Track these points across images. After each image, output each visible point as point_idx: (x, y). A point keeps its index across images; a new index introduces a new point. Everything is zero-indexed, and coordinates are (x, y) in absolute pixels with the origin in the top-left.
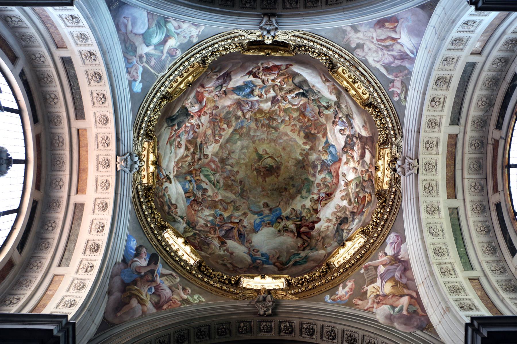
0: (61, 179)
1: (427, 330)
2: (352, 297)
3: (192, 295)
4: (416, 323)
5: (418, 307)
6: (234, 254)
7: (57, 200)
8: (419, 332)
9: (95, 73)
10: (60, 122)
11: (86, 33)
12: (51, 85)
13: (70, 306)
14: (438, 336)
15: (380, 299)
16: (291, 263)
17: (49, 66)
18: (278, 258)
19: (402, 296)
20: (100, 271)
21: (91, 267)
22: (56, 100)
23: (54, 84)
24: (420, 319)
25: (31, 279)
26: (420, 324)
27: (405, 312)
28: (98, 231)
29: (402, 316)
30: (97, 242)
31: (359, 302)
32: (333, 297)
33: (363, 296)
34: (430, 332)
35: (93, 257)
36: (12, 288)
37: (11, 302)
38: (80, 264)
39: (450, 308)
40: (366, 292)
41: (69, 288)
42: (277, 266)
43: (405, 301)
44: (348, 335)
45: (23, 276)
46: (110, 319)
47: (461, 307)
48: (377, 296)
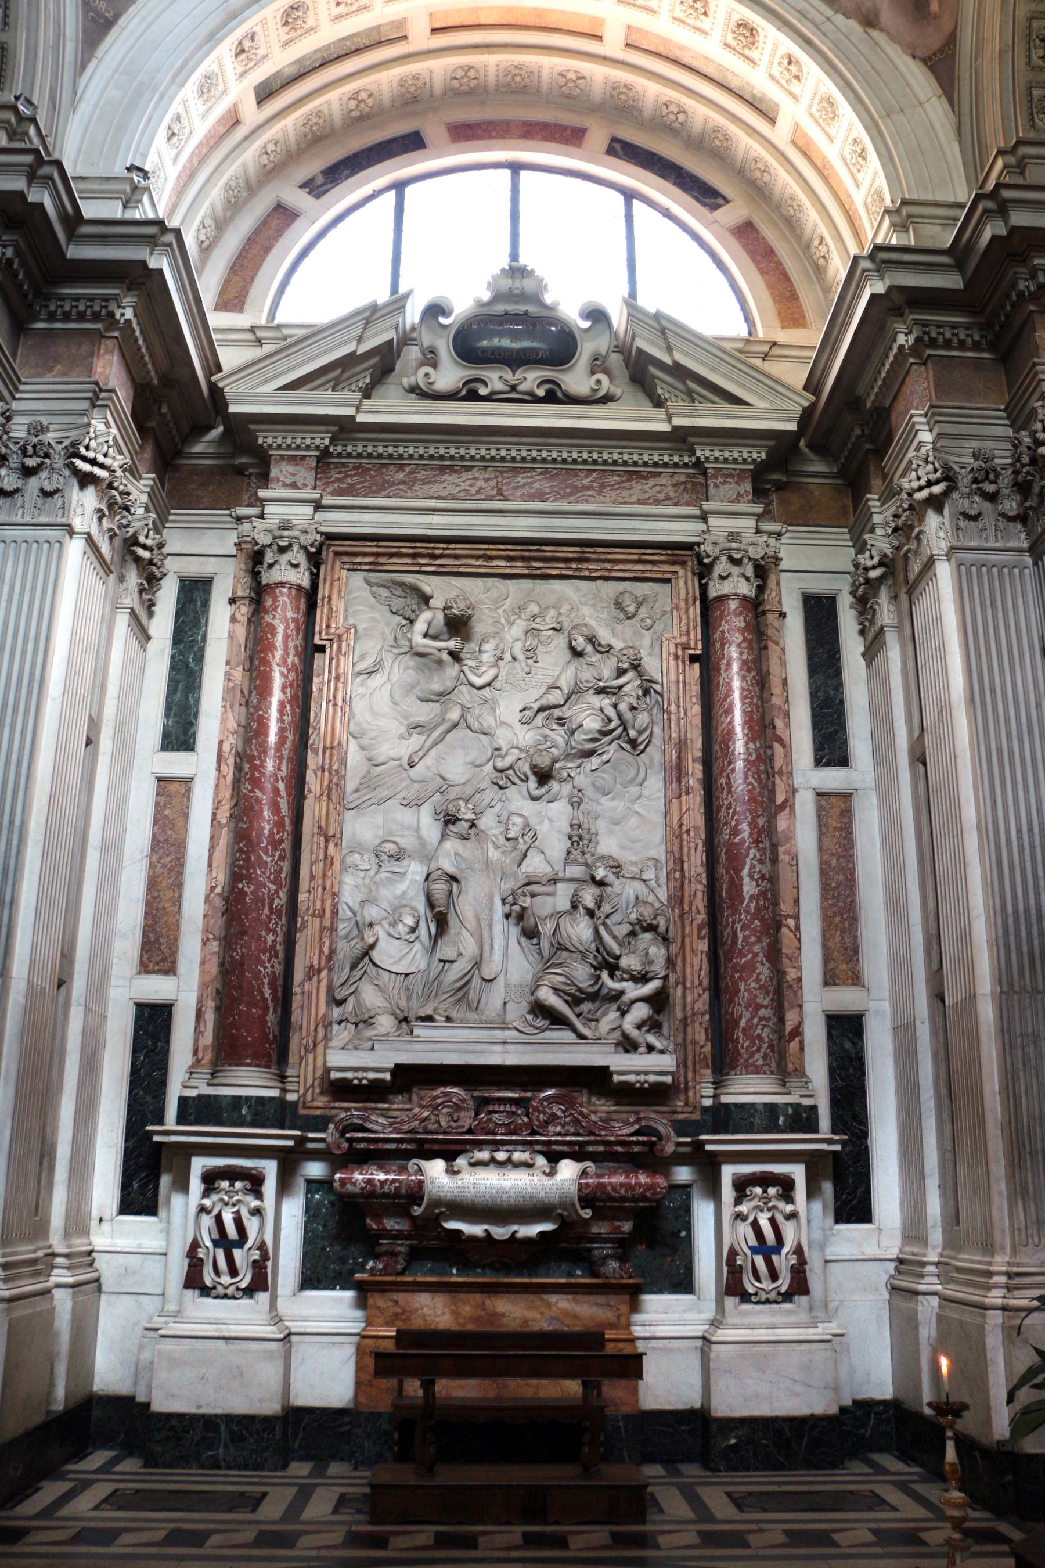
0: (560, 74)
7: (614, 89)
9: (286, 23)
10: (416, 77)
11: (195, 89)
12: (326, 112)
13: (864, 159)
17: (285, 130)
20: (807, 42)
21: (790, 63)
22: (363, 95)
23: (325, 107)
25: (786, 195)
28: (705, 14)
30: (733, 25)
35: (769, 47)
36: (799, 237)
37: (824, 257)
38: (778, 82)
41: (827, 134)
45: (778, 207)
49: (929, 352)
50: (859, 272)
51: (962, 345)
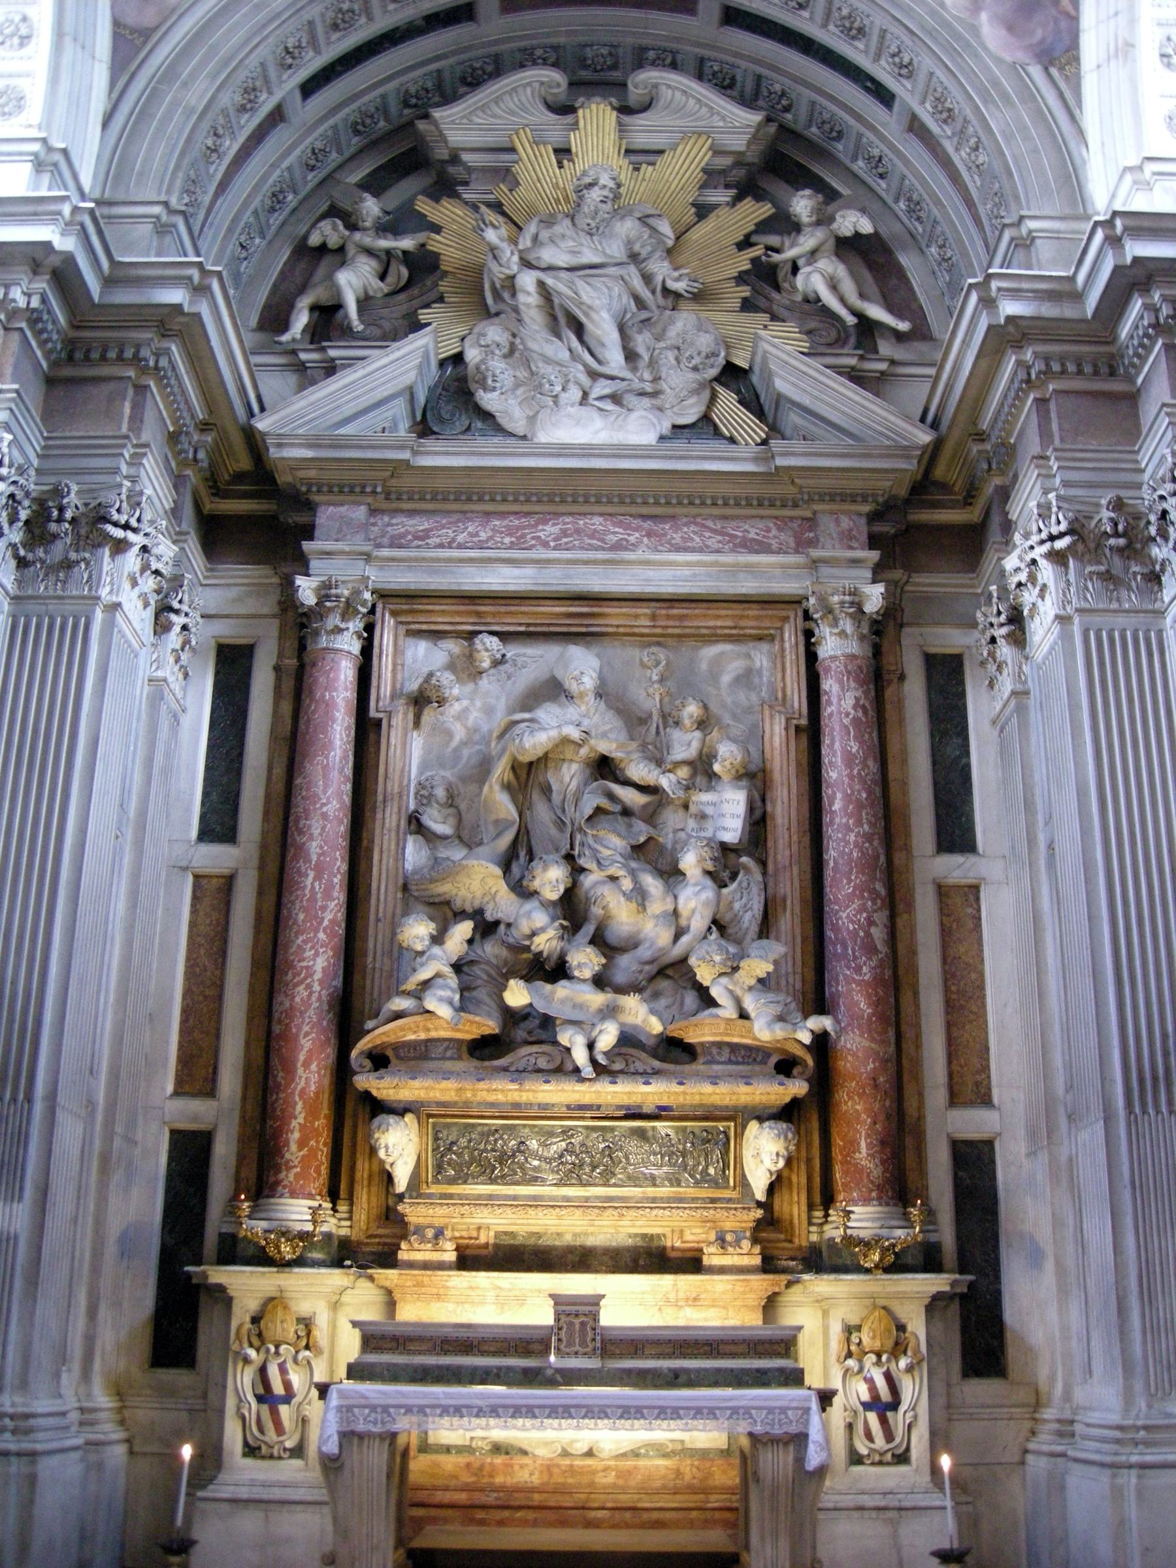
1: (1061, 69)
4: (1039, 34)
8: (1036, 71)
14: (1080, 106)
24: (1056, 21)
26: (1049, 40)
34: (1067, 79)
39: (1133, 46)
44: (845, 12)
46: (131, 19)
47: (1163, 56)
49: (24, 325)
50: (53, 207)
51: (42, 344)
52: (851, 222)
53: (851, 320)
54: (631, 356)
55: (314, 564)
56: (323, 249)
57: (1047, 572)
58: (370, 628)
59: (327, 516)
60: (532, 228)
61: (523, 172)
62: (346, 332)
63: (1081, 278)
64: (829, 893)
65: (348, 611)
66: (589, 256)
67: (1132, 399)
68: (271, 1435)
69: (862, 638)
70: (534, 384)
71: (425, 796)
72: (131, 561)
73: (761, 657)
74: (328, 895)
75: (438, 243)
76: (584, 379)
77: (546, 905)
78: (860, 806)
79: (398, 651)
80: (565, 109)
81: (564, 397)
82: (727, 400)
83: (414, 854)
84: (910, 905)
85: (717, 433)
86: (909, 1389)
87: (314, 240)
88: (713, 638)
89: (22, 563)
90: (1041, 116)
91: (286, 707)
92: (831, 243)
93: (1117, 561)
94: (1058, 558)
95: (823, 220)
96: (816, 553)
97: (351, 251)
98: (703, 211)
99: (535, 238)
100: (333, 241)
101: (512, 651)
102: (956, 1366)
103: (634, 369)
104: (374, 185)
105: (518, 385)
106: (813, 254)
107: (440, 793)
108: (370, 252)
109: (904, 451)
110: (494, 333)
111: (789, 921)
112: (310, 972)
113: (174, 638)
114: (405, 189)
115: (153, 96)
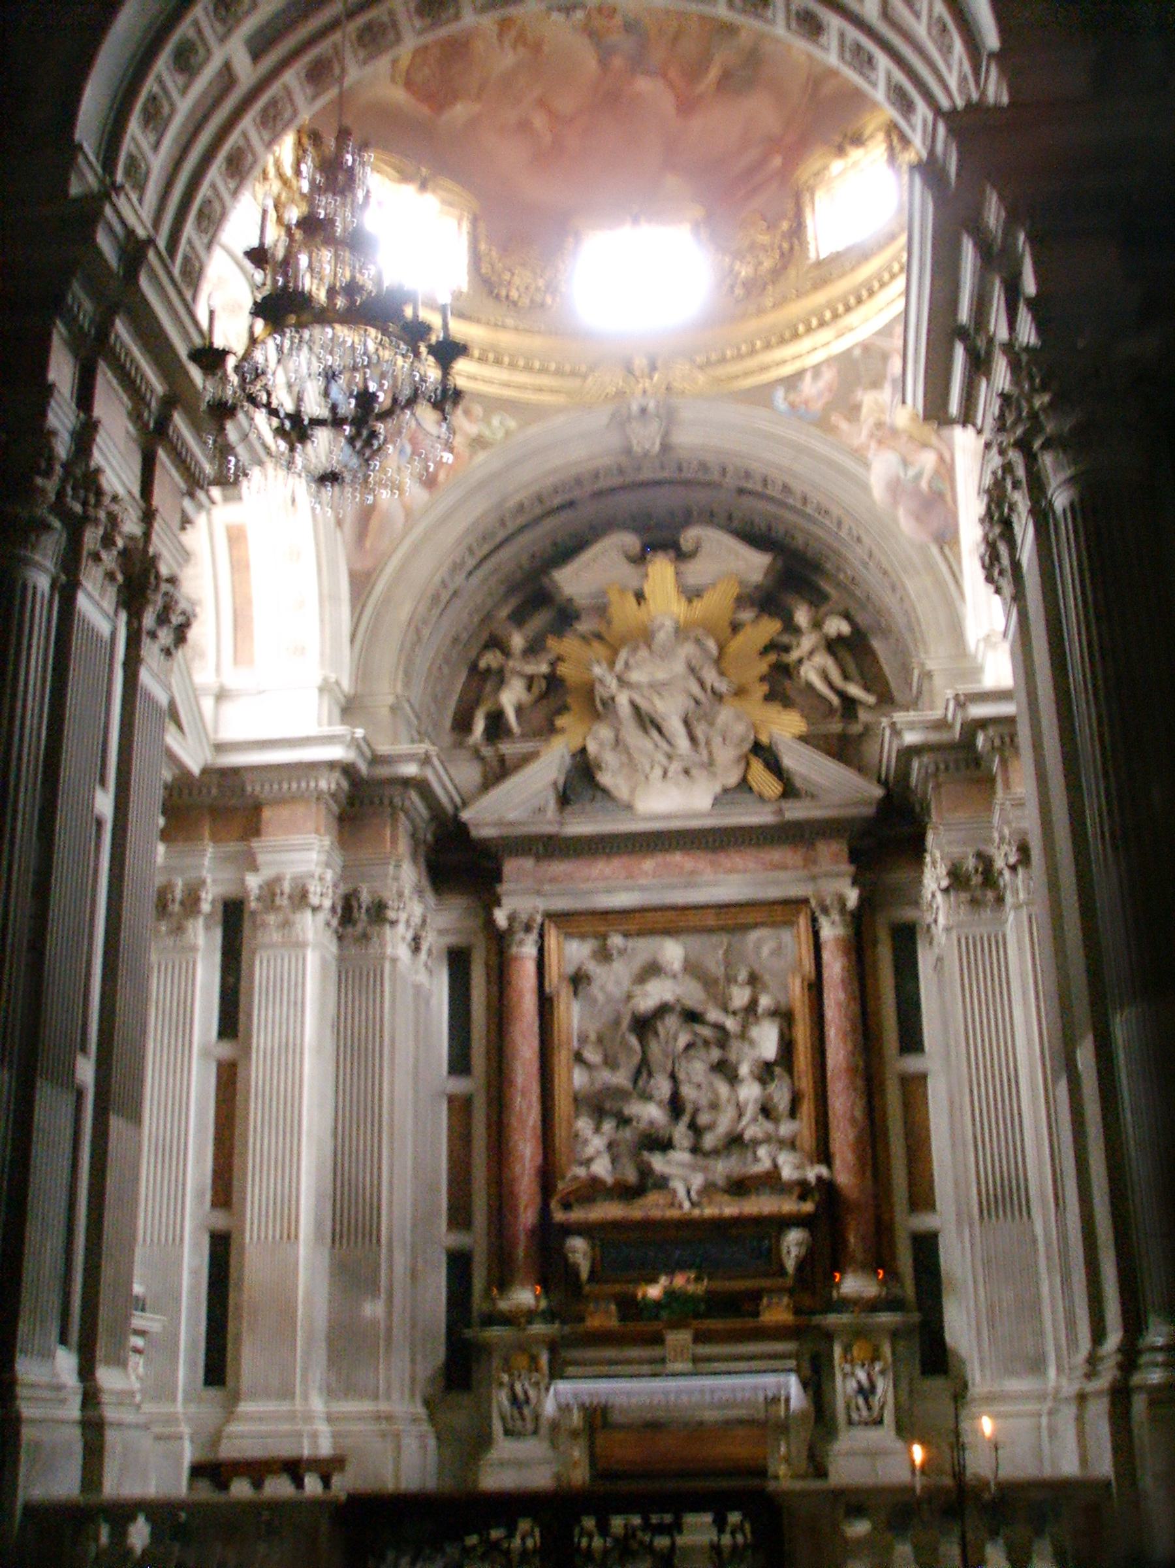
2: (829, 407)
3: (486, 420)
5: (948, 486)
6: (546, 49)
8: (935, 550)
15: (885, 433)
16: (714, 73)
18: (676, 39)
19: (925, 445)
27: (924, 485)
29: (917, 492)
31: (844, 425)
32: (792, 397)
33: (852, 413)
40: (856, 408)
42: (671, 85)
43: (927, 460)
48: (879, 425)
52: (837, 626)
53: (835, 700)
54: (693, 739)
55: (504, 901)
56: (488, 670)
57: (939, 897)
58: (541, 936)
59: (510, 867)
60: (623, 654)
61: (615, 611)
62: (508, 732)
63: (950, 716)
64: (830, 1087)
65: (528, 928)
66: (661, 675)
67: (992, 780)
68: (519, 1423)
69: (846, 925)
70: (631, 764)
71: (583, 1039)
72: (401, 927)
73: (786, 936)
74: (529, 1108)
75: (563, 670)
76: (664, 761)
77: (660, 1103)
78: (845, 1035)
79: (560, 949)
80: (639, 559)
81: (651, 776)
82: (757, 767)
83: (579, 1078)
84: (883, 1092)
85: (750, 789)
86: (880, 1384)
87: (482, 664)
88: (756, 926)
89: (340, 938)
90: (939, 583)
91: (495, 989)
92: (823, 642)
93: (978, 893)
94: (946, 891)
95: (817, 625)
96: (816, 870)
97: (508, 674)
98: (736, 627)
99: (627, 664)
100: (495, 665)
101: (631, 943)
102: (917, 1372)
103: (696, 751)
104: (518, 618)
105: (622, 765)
106: (811, 653)
107: (593, 1037)
108: (521, 674)
109: (865, 803)
110: (604, 732)
111: (807, 1108)
112: (522, 1156)
113: (423, 955)
114: (540, 620)
115: (377, 617)
